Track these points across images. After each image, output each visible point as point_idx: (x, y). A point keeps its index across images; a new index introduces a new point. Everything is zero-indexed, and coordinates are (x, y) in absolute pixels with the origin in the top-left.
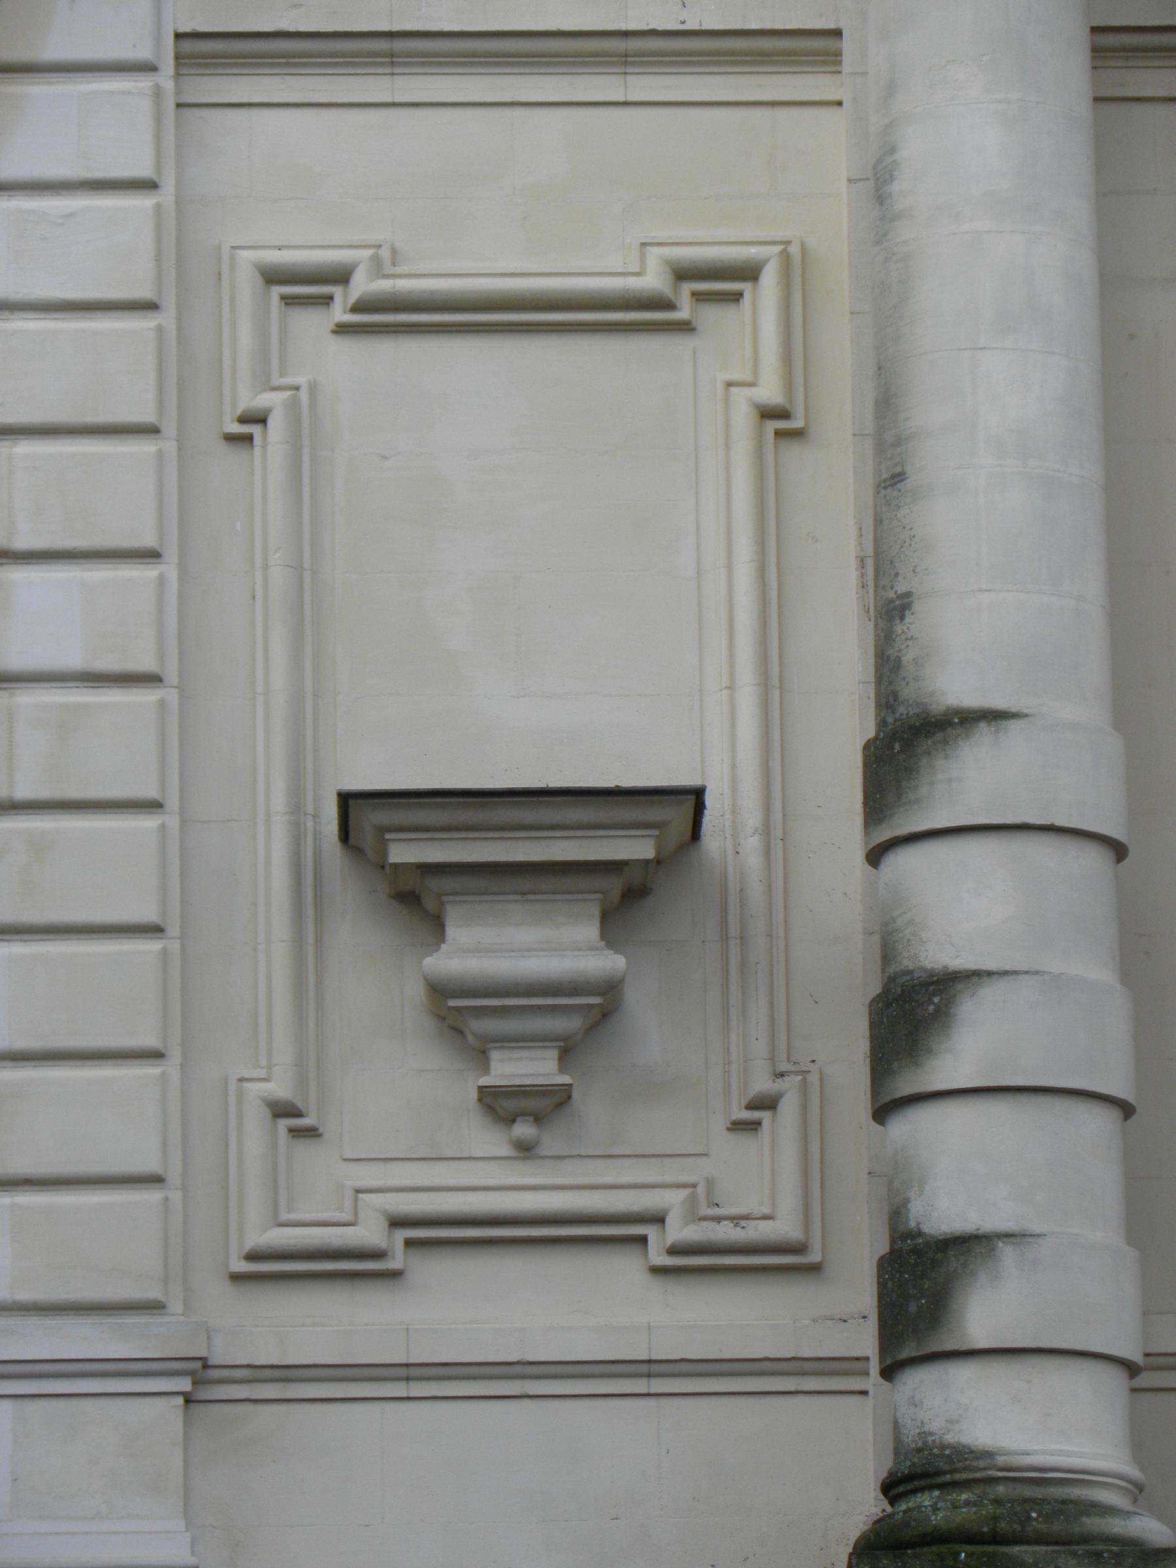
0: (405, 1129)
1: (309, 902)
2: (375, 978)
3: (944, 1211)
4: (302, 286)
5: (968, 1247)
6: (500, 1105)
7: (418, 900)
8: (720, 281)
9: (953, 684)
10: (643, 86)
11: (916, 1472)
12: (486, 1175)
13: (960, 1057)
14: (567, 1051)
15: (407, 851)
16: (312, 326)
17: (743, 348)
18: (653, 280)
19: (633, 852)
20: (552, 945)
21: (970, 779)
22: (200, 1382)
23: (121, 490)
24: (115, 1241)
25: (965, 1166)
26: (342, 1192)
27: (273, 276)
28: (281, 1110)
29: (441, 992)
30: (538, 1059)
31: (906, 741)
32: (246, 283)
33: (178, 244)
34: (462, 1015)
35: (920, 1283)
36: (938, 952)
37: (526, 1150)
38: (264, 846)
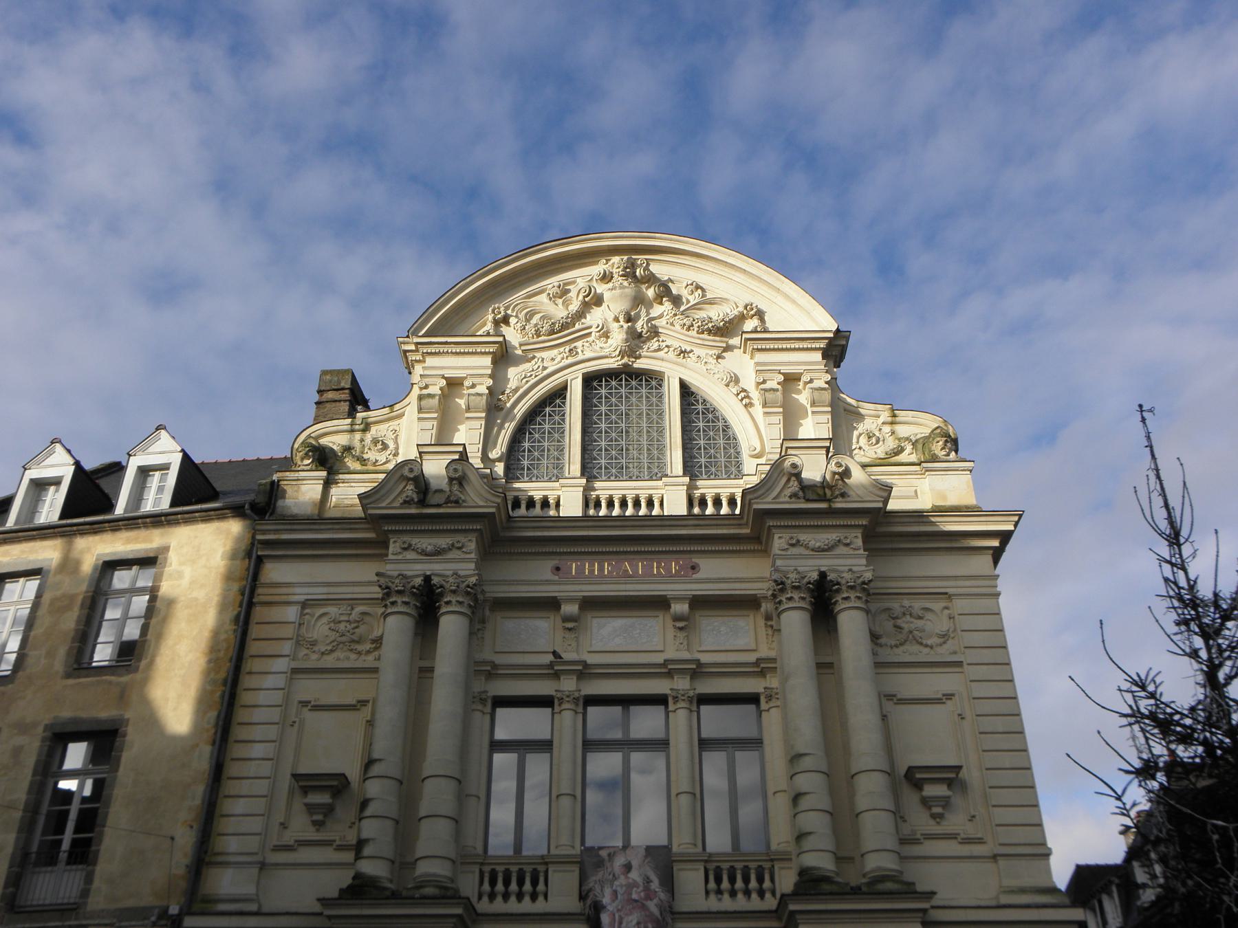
0: (301, 826)
1: (291, 793)
2: (298, 804)
3: (364, 835)
4: (304, 703)
5: (366, 841)
6: (315, 823)
7: (305, 791)
8: (363, 703)
9: (375, 756)
10: (357, 676)
11: (357, 876)
12: (311, 834)
13: (368, 812)
14: (325, 815)
15: (306, 783)
16: (305, 709)
17: (366, 713)
18: (354, 702)
19: (337, 785)
20: (323, 798)
21: (376, 770)
22: (263, 866)
23: (272, 732)
24: (253, 844)
25: (369, 828)
26: (289, 837)
27: (300, 702)
28: (282, 824)
29: (306, 805)
30: (322, 816)
31: (369, 763)
32: (296, 703)
33: (287, 698)
34: (311, 808)
35: (360, 844)
36: (368, 796)
37: (318, 830)
38: (285, 782)
